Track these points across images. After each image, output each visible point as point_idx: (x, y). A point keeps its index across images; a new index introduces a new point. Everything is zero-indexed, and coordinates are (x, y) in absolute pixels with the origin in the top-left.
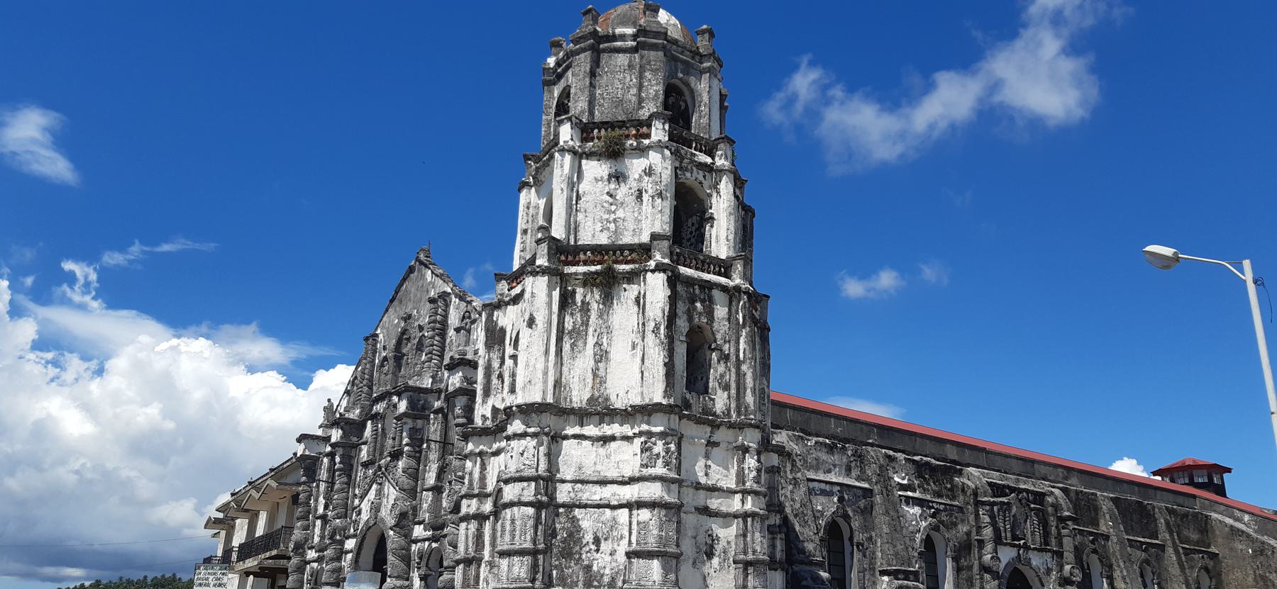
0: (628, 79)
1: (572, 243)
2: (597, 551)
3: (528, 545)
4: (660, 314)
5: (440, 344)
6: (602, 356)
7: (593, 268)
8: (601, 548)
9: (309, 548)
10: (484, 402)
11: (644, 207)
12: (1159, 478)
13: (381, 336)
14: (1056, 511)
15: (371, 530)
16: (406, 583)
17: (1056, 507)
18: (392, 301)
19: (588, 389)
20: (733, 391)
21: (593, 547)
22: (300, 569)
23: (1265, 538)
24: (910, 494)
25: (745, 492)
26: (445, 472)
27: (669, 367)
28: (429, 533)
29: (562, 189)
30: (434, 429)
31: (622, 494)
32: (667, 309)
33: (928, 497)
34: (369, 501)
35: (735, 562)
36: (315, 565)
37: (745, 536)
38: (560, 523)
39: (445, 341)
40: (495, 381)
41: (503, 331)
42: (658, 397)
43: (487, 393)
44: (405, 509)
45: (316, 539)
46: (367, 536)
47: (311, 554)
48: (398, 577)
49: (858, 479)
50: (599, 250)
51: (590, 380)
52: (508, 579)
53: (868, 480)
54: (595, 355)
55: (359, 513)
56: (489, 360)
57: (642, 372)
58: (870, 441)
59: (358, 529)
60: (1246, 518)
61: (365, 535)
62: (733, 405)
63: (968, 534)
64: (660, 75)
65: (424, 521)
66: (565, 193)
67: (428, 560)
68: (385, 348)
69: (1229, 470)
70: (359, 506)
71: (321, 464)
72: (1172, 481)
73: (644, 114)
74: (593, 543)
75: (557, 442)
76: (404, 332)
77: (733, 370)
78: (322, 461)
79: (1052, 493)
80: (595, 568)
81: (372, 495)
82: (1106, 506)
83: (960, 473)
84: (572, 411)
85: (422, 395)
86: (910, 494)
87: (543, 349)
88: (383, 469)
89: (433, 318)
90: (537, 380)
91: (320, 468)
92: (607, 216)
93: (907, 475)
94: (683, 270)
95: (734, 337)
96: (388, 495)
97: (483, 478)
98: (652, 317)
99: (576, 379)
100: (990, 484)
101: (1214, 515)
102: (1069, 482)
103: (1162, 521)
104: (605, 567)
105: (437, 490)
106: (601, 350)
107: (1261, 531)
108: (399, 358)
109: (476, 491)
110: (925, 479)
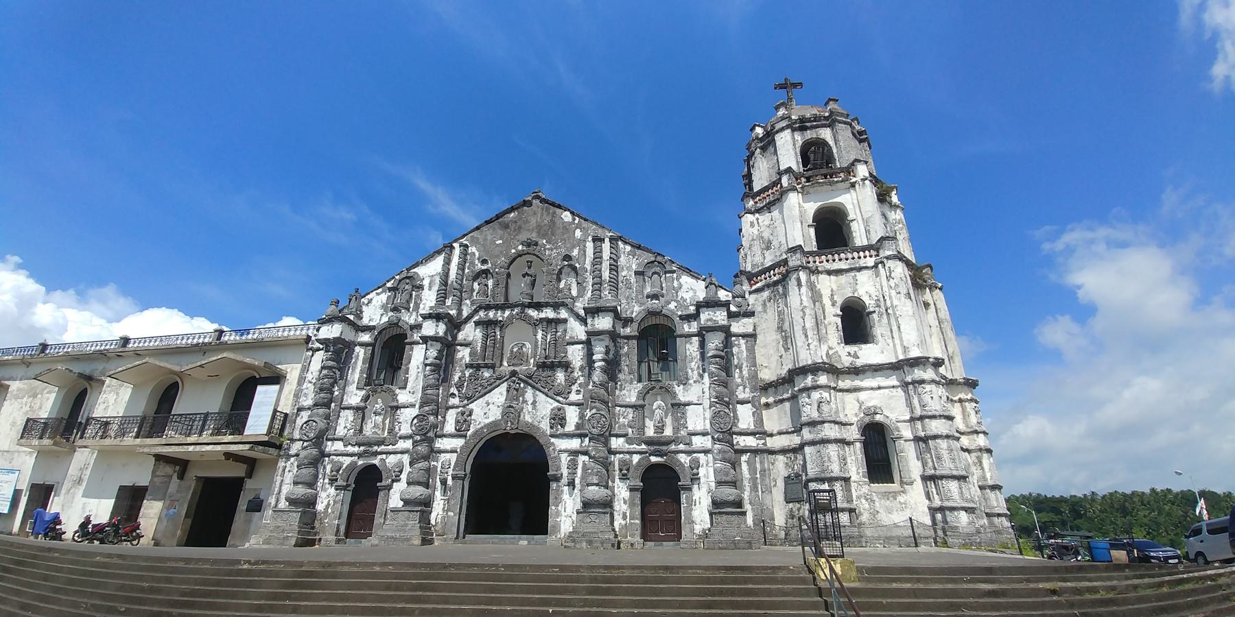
18: (487, 222)
45: (341, 431)
59: (468, 430)
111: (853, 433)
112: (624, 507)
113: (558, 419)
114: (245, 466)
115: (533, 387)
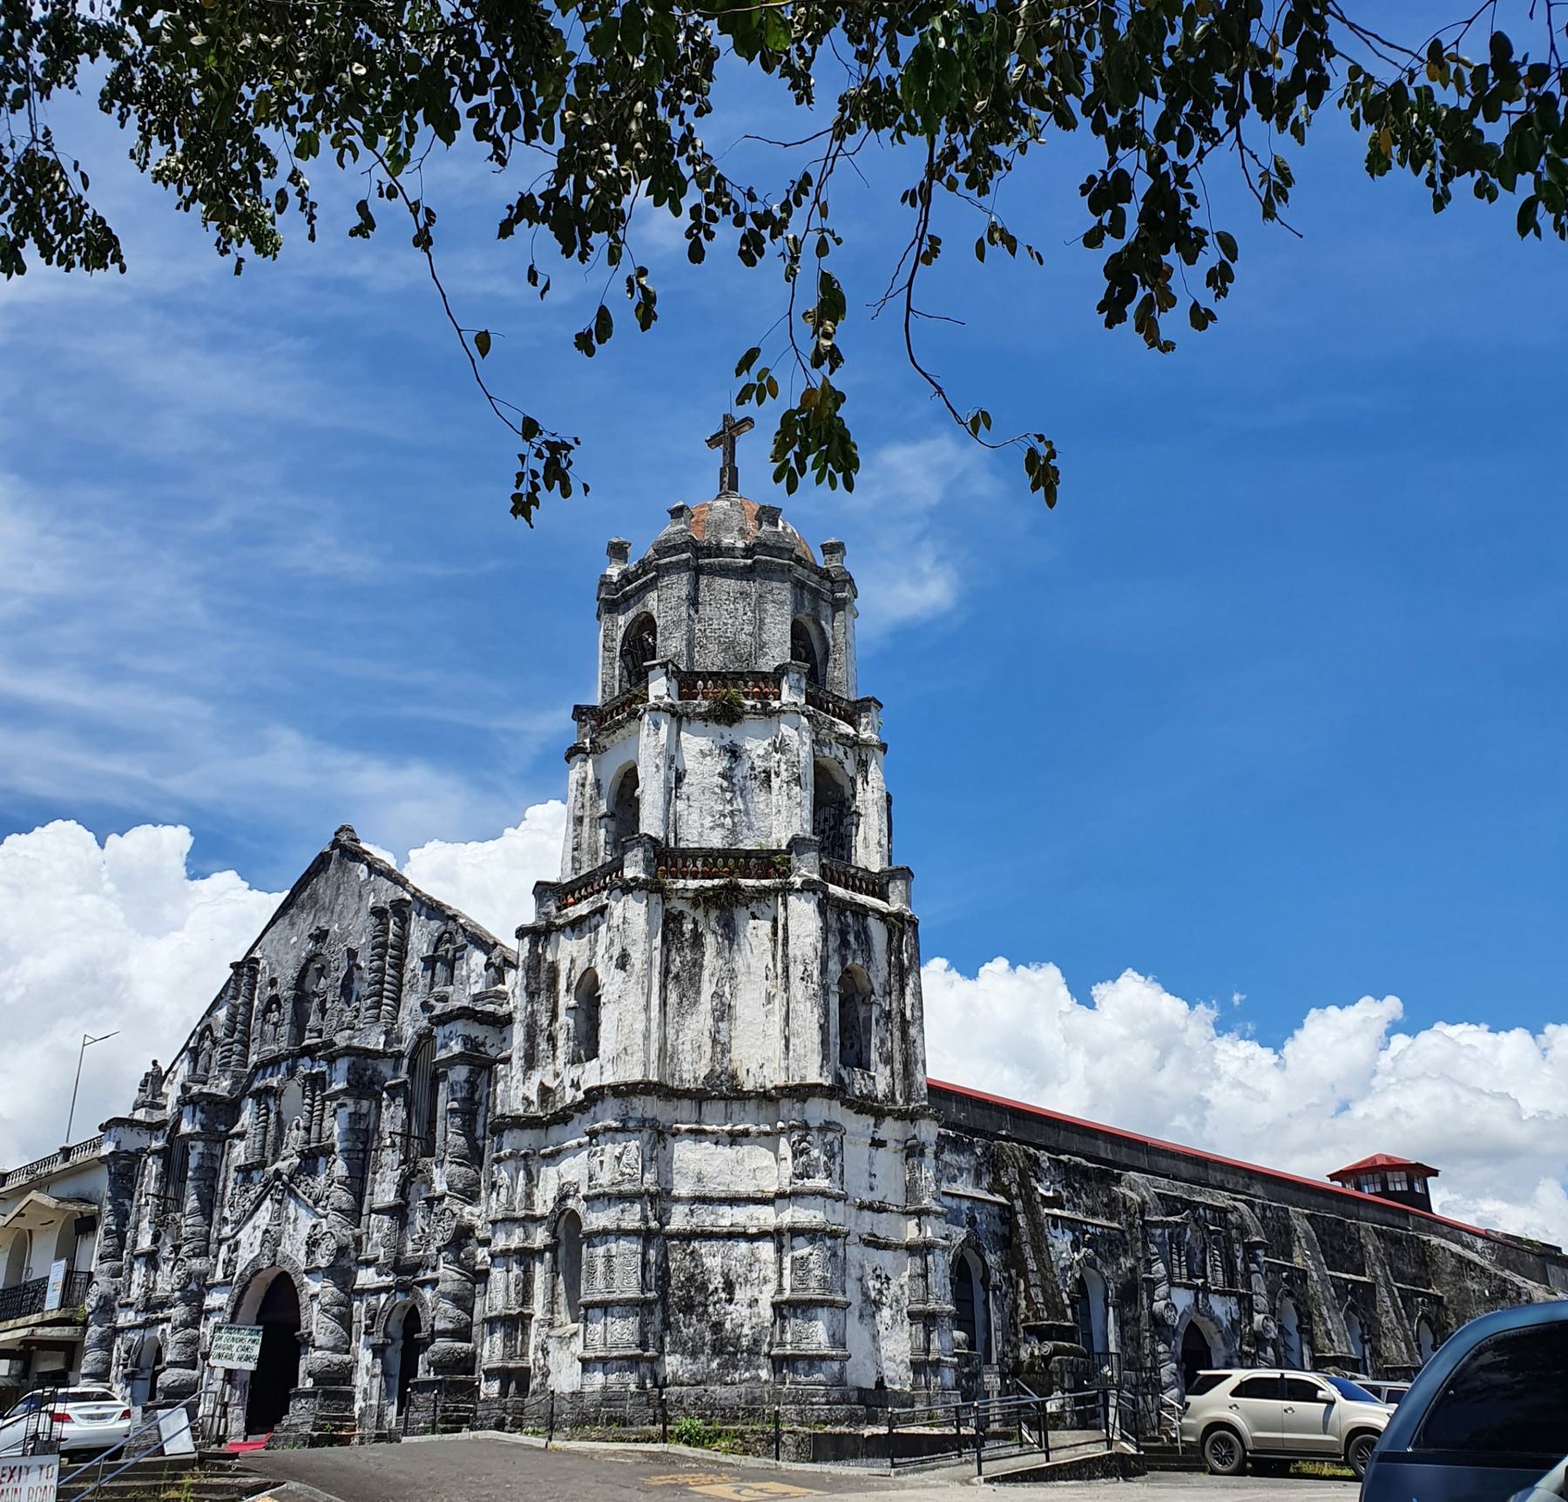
0: (741, 611)
1: (672, 844)
2: (730, 1301)
3: (633, 1293)
4: (811, 954)
5: (395, 981)
6: (723, 1012)
7: (708, 883)
8: (736, 1297)
9: (121, 1306)
10: (526, 1077)
11: (774, 798)
12: (1339, 1184)
13: (263, 963)
14: (1242, 1234)
15: (259, 1276)
16: (347, 1358)
17: (1244, 1230)
19: (705, 1060)
20: (898, 1066)
21: (723, 1295)
22: (106, 1343)
23: (1507, 1273)
24: (1057, 1211)
25: (921, 1213)
26: (412, 1183)
27: (823, 1029)
28: (388, 1280)
29: (657, 766)
30: (392, 1117)
31: (762, 1217)
32: (819, 946)
33: (1080, 1217)
34: (254, 1228)
35: (910, 1314)
36: (135, 1336)
37: (925, 1276)
38: (675, 1260)
39: (402, 975)
40: (543, 1045)
41: (553, 969)
42: (813, 1073)
43: (530, 1062)
44: (345, 1241)
46: (251, 1285)
47: (125, 1318)
48: (335, 1349)
49: (991, 1191)
50: (711, 860)
51: (707, 1048)
52: (605, 1344)
53: (1005, 1191)
54: (714, 1010)
55: (235, 1248)
56: (533, 1013)
57: (787, 1040)
58: (1004, 1133)
59: (234, 1274)
60: (1480, 1243)
61: (250, 1281)
62: (898, 1087)
63: (1133, 1270)
64: (787, 609)
65: (377, 1259)
66: (662, 771)
67: (388, 1320)
68: (273, 983)
69: (1435, 1173)
70: (234, 1236)
71: (144, 1168)
72: (1359, 1188)
73: (768, 664)
74: (724, 1290)
75: (664, 1140)
76: (311, 959)
77: (897, 1034)
78: (146, 1162)
79: (1235, 1208)
80: (728, 1326)
81: (263, 1217)
82: (1301, 1226)
83: (1118, 1180)
84: (686, 1094)
85: (369, 1061)
86: (1057, 1211)
87: (642, 1001)
88: (285, 1178)
89: (381, 939)
90: (636, 1048)
91: (143, 1175)
92: (721, 808)
93: (1052, 1183)
94: (834, 889)
95: (897, 986)
96: (296, 1219)
97: (529, 1196)
98: (799, 958)
99: (688, 1047)
100: (1158, 1195)
101: (1435, 1241)
102: (1252, 1192)
103: (1370, 1248)
104: (742, 1325)
105: (399, 1213)
106: (723, 1004)
107: (1503, 1262)
108: (301, 996)
109: (520, 1213)
110: (1074, 1189)
111: (540, 1237)
112: (367, 1379)
113: (313, 1244)
114: (62, 1354)
115: (296, 1196)
